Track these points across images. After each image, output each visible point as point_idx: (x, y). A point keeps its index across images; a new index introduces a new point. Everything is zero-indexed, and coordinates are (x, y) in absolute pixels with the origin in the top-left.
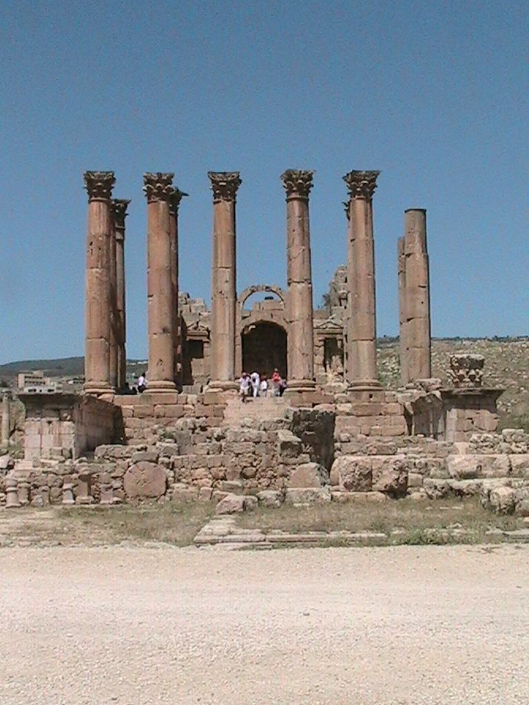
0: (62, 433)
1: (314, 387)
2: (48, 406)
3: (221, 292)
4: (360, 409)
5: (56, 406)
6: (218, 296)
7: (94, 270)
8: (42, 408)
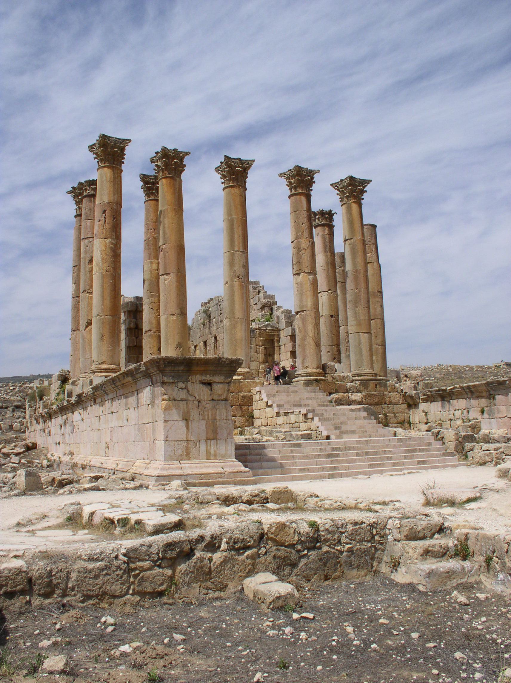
1: (324, 376)
2: (198, 377)
3: (238, 277)
6: (236, 280)
7: (108, 241)
8: (187, 381)
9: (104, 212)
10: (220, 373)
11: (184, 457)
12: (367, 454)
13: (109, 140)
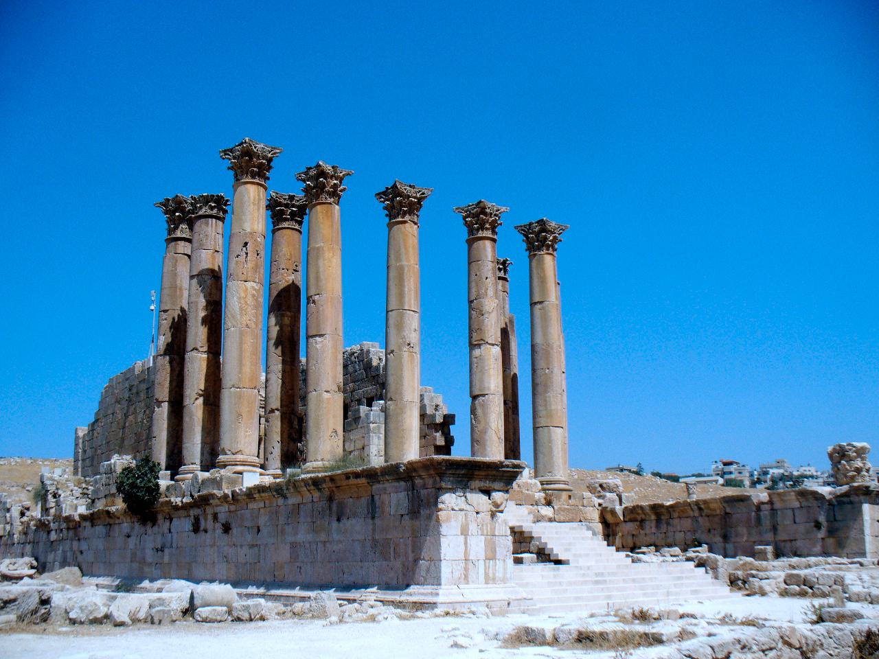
0: (497, 534)
4: (562, 513)
5: (487, 484)
7: (249, 284)
9: (246, 244)
10: (500, 480)
11: (462, 580)
12: (634, 581)
13: (255, 147)
